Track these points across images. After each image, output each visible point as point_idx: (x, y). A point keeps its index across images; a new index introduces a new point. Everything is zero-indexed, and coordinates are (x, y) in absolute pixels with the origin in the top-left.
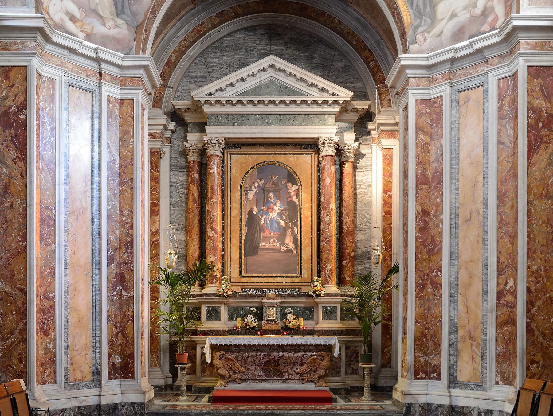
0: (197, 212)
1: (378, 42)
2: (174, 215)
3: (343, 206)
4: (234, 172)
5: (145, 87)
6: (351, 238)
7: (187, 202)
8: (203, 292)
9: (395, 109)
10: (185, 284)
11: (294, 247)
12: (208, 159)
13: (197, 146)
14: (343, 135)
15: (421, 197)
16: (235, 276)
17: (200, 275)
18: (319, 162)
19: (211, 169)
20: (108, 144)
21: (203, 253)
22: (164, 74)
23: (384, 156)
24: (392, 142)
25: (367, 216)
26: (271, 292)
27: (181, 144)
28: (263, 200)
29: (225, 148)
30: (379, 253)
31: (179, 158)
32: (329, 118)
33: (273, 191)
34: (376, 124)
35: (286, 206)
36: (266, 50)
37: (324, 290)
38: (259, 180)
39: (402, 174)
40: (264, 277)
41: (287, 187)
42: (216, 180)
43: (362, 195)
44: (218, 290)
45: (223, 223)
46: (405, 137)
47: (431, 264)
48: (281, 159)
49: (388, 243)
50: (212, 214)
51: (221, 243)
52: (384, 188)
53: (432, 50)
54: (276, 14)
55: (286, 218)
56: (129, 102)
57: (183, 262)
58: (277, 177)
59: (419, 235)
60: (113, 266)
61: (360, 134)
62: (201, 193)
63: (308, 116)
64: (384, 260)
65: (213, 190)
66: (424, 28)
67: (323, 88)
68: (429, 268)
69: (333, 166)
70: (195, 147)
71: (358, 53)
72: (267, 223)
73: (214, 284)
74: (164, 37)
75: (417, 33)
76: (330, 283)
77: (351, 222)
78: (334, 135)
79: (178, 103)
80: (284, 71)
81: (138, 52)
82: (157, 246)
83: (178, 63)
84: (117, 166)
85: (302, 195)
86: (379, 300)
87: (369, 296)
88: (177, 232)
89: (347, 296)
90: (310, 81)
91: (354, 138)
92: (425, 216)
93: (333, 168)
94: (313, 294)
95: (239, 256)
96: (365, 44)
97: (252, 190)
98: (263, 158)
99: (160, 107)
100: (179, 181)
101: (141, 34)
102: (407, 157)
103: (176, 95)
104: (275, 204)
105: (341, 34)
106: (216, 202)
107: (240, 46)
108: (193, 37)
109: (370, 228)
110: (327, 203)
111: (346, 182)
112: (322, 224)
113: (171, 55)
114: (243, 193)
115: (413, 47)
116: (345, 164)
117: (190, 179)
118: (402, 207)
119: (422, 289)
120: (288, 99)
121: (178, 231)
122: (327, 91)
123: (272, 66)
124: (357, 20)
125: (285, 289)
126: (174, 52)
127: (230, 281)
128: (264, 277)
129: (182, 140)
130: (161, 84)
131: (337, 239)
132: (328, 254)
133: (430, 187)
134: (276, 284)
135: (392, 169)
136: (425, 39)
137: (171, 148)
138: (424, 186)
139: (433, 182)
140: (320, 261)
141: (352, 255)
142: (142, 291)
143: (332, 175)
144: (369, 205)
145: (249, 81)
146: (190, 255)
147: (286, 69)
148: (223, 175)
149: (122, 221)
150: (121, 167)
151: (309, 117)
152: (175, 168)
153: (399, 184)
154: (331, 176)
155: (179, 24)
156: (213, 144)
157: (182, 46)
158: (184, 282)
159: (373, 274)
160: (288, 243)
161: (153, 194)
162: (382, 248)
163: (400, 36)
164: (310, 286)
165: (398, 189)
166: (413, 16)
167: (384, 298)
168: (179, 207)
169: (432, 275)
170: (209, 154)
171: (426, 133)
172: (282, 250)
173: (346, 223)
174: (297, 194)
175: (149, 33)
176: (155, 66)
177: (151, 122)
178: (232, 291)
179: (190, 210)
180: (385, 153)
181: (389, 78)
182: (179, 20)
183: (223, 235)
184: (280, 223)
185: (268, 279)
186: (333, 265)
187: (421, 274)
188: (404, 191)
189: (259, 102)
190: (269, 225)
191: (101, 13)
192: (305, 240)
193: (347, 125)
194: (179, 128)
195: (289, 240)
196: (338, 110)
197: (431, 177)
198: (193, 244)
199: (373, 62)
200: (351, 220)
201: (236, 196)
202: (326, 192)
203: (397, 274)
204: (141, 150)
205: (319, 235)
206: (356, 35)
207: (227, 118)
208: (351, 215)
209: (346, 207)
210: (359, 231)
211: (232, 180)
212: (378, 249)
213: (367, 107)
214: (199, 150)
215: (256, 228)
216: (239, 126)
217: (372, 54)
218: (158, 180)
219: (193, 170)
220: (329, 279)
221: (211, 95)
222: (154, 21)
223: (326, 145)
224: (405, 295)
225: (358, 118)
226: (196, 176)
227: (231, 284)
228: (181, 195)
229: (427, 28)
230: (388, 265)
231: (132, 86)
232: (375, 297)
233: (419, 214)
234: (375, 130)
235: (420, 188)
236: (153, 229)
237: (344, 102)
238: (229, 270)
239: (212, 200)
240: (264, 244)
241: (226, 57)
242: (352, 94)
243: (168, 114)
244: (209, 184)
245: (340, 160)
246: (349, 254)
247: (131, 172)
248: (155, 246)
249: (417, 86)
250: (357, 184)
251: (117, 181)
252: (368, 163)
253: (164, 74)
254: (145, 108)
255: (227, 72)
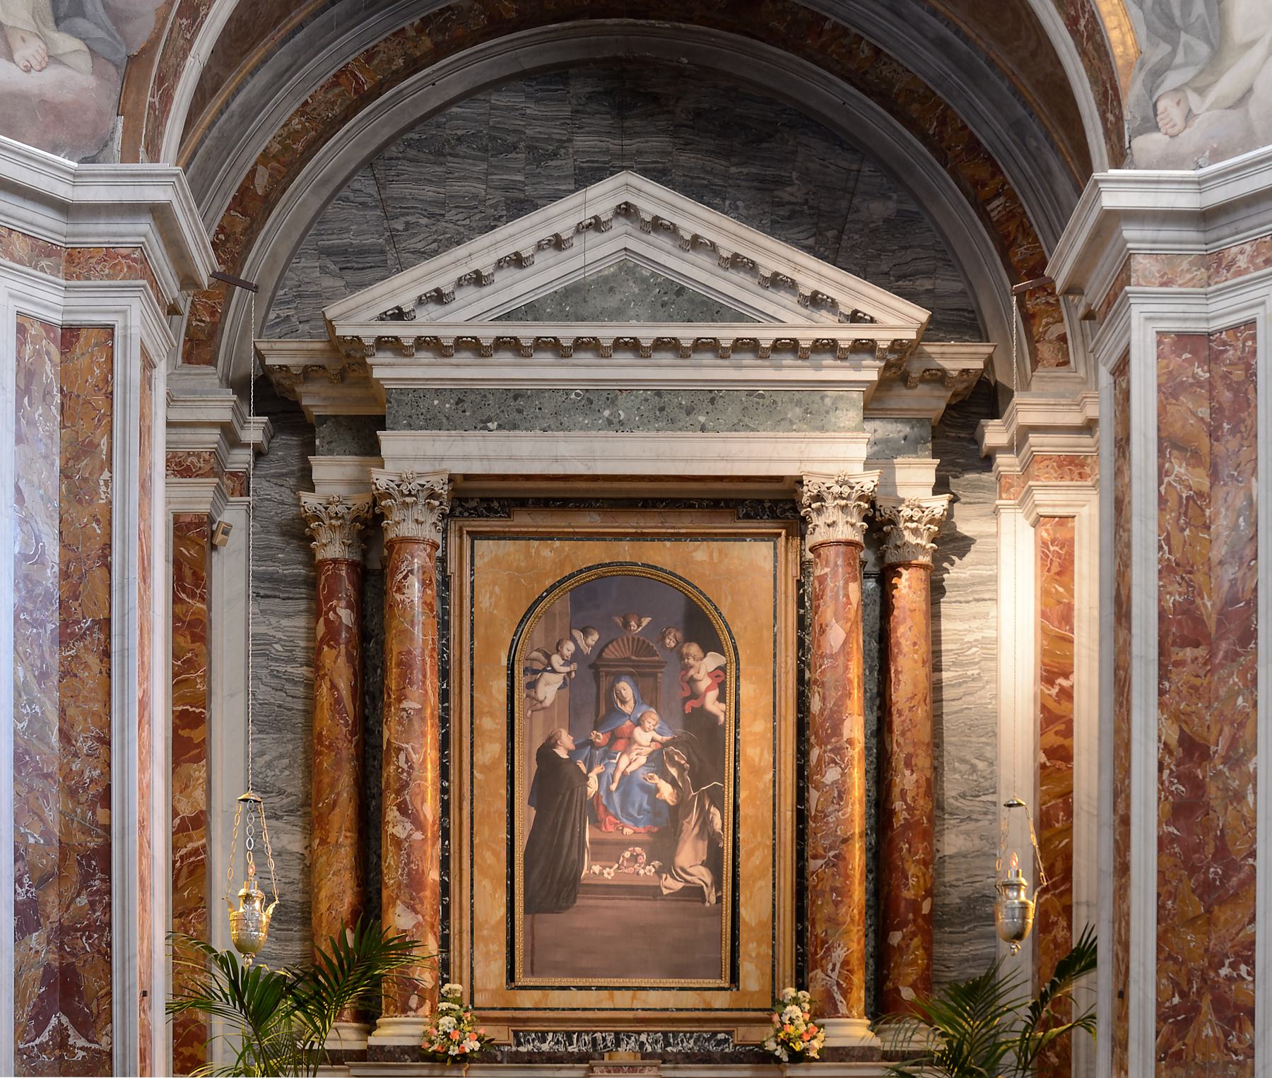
0: (347, 749)
1: (1018, 128)
2: (261, 761)
3: (890, 731)
4: (484, 601)
5: (154, 283)
6: (921, 846)
7: (310, 713)
8: (373, 1040)
9: (1082, 373)
10: (305, 1012)
11: (708, 879)
12: (391, 553)
13: (350, 503)
14: (892, 468)
15: (1179, 692)
16: (491, 986)
17: (360, 979)
18: (804, 566)
19: (399, 590)
20: (18, 490)
21: (369, 900)
22: (227, 240)
23: (1045, 544)
24: (1072, 495)
25: (981, 765)
26: (623, 1045)
27: (287, 496)
28: (593, 709)
29: (452, 515)
30: (1023, 898)
31: (282, 550)
32: (840, 405)
33: (631, 675)
34: (1013, 428)
35: (680, 730)
36: (606, 152)
37: (821, 1035)
38: (578, 635)
39: (1110, 609)
40: (599, 988)
41: (682, 657)
42: (418, 631)
43: (961, 691)
44: (425, 1034)
45: (445, 791)
46: (1118, 473)
47: (1213, 936)
48: (661, 555)
49: (1059, 865)
50: (402, 757)
51: (436, 864)
52: (1043, 664)
53: (1217, 156)
54: (642, 22)
55: (681, 775)
56: (94, 337)
57: (296, 931)
58: (646, 621)
59: (1172, 829)
60: (35, 939)
61: (954, 464)
62: (363, 681)
63: (762, 396)
64: (1044, 923)
65: (405, 666)
66: (1186, 75)
67: (816, 293)
68: (1207, 950)
69: (854, 579)
70: (341, 509)
71: (944, 166)
72: (609, 792)
73: (412, 1013)
74: (227, 104)
75: (1160, 92)
76: (843, 1009)
77: (922, 790)
78: (858, 468)
79: (278, 346)
80: (671, 230)
81: (129, 155)
82: (199, 871)
83: (277, 201)
84: (50, 576)
85: (737, 688)
86: (1025, 1069)
87: (988, 1059)
88: (274, 822)
89: (904, 1056)
90: (769, 265)
91: (933, 480)
92: (1191, 759)
93: (854, 589)
94: (779, 1052)
95: (502, 911)
96: (971, 135)
97: (554, 671)
98: (594, 553)
99: (212, 362)
100: (280, 635)
101: (141, 90)
102: (1128, 545)
103: (272, 316)
104: (639, 723)
105: (883, 97)
106: (419, 711)
107: (511, 139)
108: (334, 103)
109: (992, 808)
110: (831, 717)
111: (902, 641)
112: (814, 795)
113: (253, 171)
114: (521, 680)
115: (1144, 145)
116: (899, 575)
117: (321, 629)
118: (1109, 727)
119: (1182, 1028)
120: (686, 333)
121: (277, 818)
122: (832, 305)
123: (626, 211)
124: (943, 45)
125: (675, 1034)
126: (265, 157)
127: (472, 1002)
128: (599, 988)
129: (291, 481)
130: (214, 275)
131: (868, 850)
132: (836, 904)
133: (1212, 654)
134: (641, 1014)
135: (1070, 592)
136: (1189, 116)
137: (253, 512)
138: (1189, 652)
139: (1221, 637)
140: (804, 929)
141: (926, 907)
142: (143, 1036)
143: (852, 615)
144: (988, 728)
145: (543, 265)
146: (323, 907)
147: (677, 221)
148: (446, 612)
149: (68, 775)
150: (65, 575)
151: (767, 402)
152: (267, 585)
153: (1096, 648)
154: (847, 620)
155: (281, 58)
156: (408, 500)
157: (294, 135)
158: (301, 1005)
159: (1002, 973)
160: (686, 866)
161: (186, 680)
162: (1037, 882)
163: (1099, 104)
164: (769, 1021)
165: (1096, 665)
166: (1143, 31)
167: (1043, 1064)
168: (280, 731)
169: (1218, 975)
170: (391, 535)
171: (1194, 457)
172: (665, 892)
173: (903, 793)
174: (722, 687)
175: (173, 87)
176: (193, 205)
177: (177, 416)
178: (480, 1039)
179: (320, 742)
180: (1045, 535)
181: (1061, 254)
182: (284, 42)
183: (445, 835)
184: (657, 790)
185: (612, 998)
186: (854, 946)
187: (1177, 973)
188: (1117, 668)
189: (580, 345)
190: (616, 798)
192: (751, 853)
193: (906, 430)
194: (281, 440)
195: (690, 856)
196: (873, 376)
197: (1214, 617)
198: (335, 868)
199: (1002, 200)
200: (923, 782)
201: (494, 692)
202: (829, 678)
203: (1092, 975)
204: (141, 515)
205: (801, 835)
206: (939, 102)
207: (460, 401)
208: (923, 761)
209: (903, 734)
210: (950, 822)
211: (480, 631)
212: (1019, 885)
213: (979, 365)
214: (356, 519)
215: (568, 810)
216: (505, 432)
217: (996, 171)
218: (204, 630)
219: (332, 595)
220: (838, 997)
221: (399, 315)
222: (191, 42)
223: (830, 503)
224: (1118, 1050)
225: (949, 407)
226: (345, 615)
227: (477, 1013)
228: (288, 686)
229: (1196, 76)
230: (1057, 946)
231: (109, 277)
232: (1010, 1058)
233: (1170, 753)
234: (1008, 449)
235: (1174, 658)
236: (186, 810)
237: (897, 346)
238: (466, 961)
239: (405, 705)
240: (596, 869)
241: (459, 179)
242: (923, 315)
243: (239, 386)
244: (394, 647)
245: (881, 558)
246: (915, 906)
247: (102, 595)
248: (191, 873)
249: (1161, 285)
250: (944, 647)
251: (50, 626)
252: (983, 571)
253: (227, 240)
254: (156, 359)
255: (459, 233)
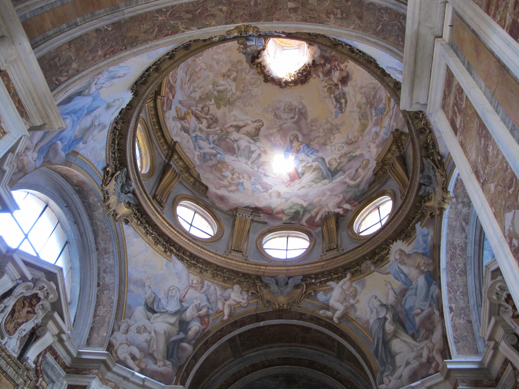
136: (390, 381)
191: (155, 356)
